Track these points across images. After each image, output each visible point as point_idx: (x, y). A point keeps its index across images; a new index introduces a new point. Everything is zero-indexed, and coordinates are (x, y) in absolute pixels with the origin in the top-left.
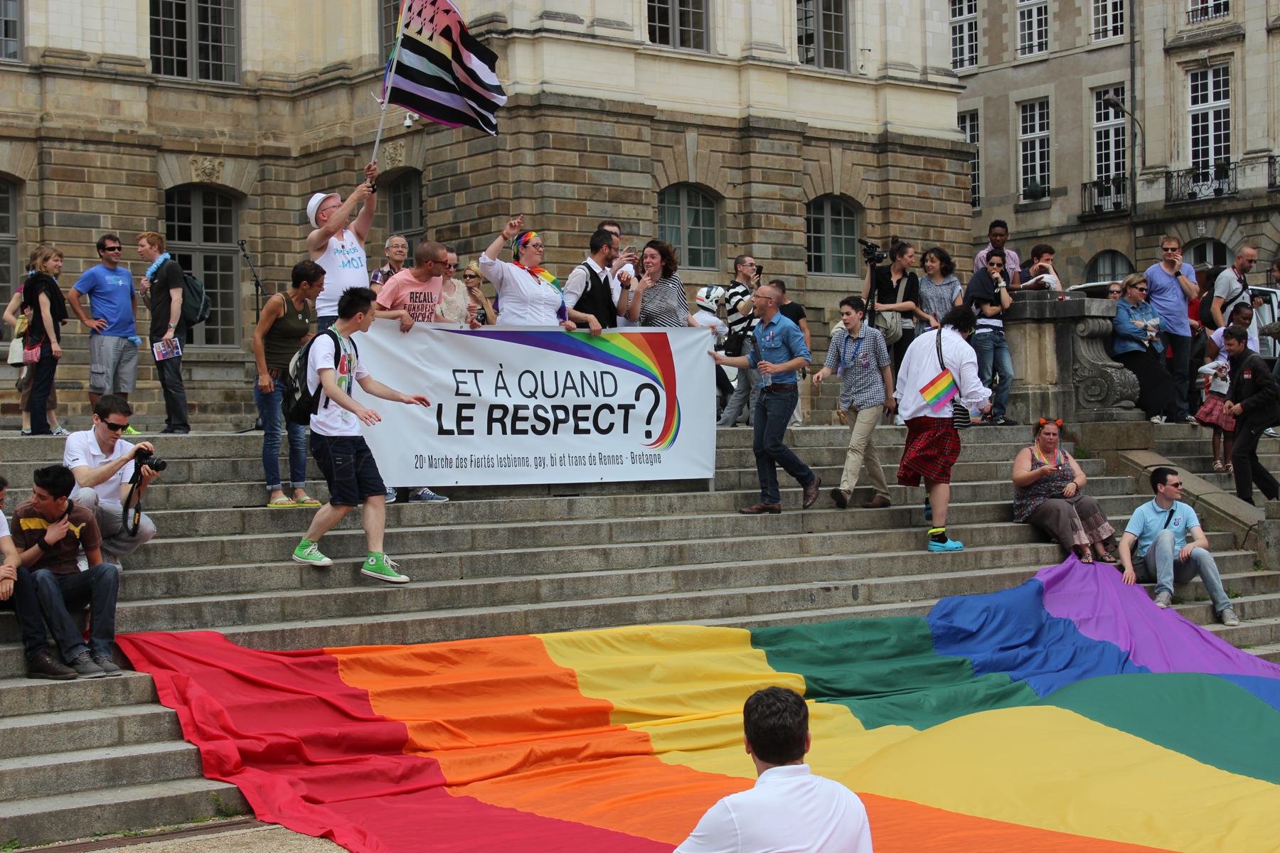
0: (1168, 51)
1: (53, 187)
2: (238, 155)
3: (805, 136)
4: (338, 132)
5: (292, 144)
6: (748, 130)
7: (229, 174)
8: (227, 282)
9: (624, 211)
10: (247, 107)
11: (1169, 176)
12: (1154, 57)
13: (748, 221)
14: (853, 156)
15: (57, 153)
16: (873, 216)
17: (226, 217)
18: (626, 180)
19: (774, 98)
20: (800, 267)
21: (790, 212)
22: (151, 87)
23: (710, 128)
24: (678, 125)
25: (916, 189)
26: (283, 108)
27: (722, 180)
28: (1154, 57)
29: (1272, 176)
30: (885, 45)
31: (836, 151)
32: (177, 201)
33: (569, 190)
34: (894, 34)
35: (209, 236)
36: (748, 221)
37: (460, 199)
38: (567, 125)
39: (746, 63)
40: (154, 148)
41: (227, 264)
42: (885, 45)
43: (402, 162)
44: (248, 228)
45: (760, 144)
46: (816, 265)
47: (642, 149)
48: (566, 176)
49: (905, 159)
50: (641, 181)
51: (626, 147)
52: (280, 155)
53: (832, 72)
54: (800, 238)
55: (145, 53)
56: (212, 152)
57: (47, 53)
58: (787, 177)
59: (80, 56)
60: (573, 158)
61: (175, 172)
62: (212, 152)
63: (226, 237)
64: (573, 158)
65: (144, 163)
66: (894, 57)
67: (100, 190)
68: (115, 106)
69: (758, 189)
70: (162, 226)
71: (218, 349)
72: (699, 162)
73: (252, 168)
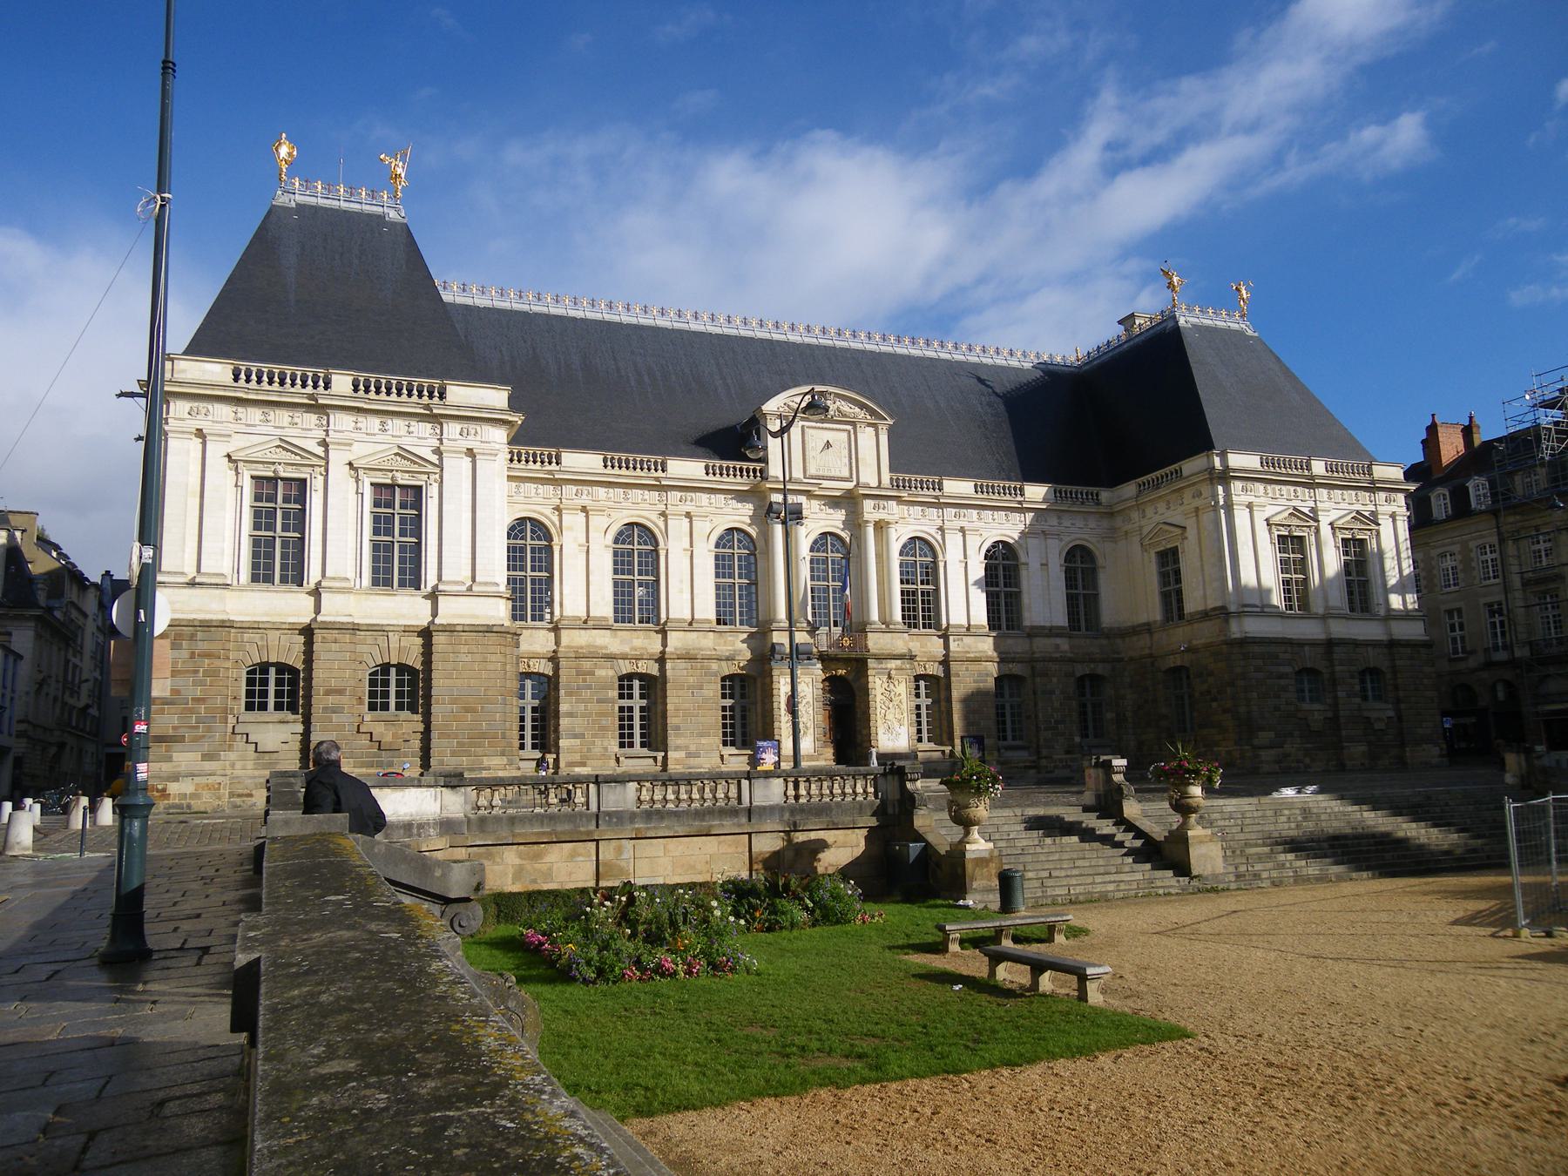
1: (1038, 680)
2: (1103, 661)
4: (1147, 651)
6: (1330, 644)
7: (1100, 669)
9: (1283, 682)
10: (1104, 642)
15: (1039, 666)
16: (1389, 676)
19: (1339, 629)
20: (1358, 700)
21: (1352, 677)
23: (1313, 644)
26: (1119, 641)
35: (1092, 695)
37: (1211, 680)
38: (1257, 649)
39: (1324, 618)
40: (1071, 660)
43: (1179, 663)
46: (1365, 698)
47: (1287, 656)
50: (1288, 669)
52: (1120, 660)
54: (1357, 688)
57: (1032, 628)
59: (1043, 628)
60: (1260, 662)
61: (1081, 670)
62: (1092, 661)
64: (1260, 662)
67: (1055, 680)
68: (1057, 646)
69: (1338, 668)
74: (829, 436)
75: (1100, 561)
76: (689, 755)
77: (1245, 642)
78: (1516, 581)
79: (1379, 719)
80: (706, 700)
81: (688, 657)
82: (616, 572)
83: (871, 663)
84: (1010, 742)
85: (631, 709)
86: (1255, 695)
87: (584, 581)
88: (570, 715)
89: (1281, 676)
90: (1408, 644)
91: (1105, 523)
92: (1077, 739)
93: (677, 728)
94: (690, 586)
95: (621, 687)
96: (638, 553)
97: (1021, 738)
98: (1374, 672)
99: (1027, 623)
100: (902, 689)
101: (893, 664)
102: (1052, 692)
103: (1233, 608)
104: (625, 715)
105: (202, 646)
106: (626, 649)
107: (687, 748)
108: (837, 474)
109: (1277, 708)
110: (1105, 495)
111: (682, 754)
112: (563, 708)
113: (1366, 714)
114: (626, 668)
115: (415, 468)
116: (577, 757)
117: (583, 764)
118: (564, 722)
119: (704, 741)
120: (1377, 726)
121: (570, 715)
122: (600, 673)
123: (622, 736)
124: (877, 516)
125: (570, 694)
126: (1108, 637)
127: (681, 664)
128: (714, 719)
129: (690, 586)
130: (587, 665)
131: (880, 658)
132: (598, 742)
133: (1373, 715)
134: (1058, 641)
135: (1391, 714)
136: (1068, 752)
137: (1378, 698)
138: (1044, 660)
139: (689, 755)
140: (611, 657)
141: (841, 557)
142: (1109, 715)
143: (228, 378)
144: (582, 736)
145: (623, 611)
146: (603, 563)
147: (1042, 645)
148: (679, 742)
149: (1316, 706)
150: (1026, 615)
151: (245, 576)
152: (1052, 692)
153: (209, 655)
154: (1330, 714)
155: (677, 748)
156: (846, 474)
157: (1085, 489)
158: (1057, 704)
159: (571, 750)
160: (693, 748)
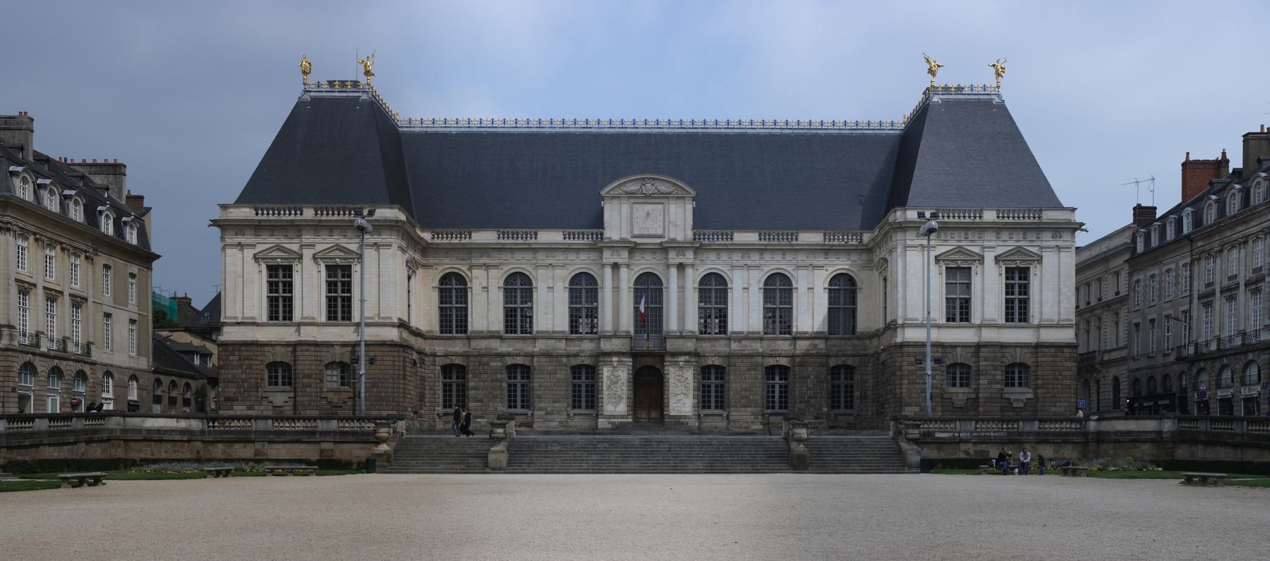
0: (1199, 298)
2: (853, 356)
3: (1003, 346)
5: (870, 351)
6: (979, 346)
7: (850, 362)
10: (856, 342)
11: (1196, 345)
12: (1195, 301)
13: (978, 373)
14: (1024, 350)
17: (852, 373)
21: (995, 369)
22: (827, 339)
23: (965, 346)
24: (953, 346)
26: (867, 342)
27: (970, 361)
28: (1195, 301)
29: (1218, 345)
30: (1041, 313)
31: (1018, 350)
32: (835, 371)
34: (1045, 310)
36: (978, 373)
38: (911, 350)
42: (1041, 313)
44: (857, 377)
45: (983, 350)
48: (910, 364)
49: (1046, 350)
52: (866, 355)
53: (1023, 324)
55: (826, 329)
56: (846, 356)
61: (833, 362)
62: (846, 356)
65: (824, 360)
66: (1045, 317)
71: (849, 411)
72: (960, 356)
73: (858, 359)
74: (649, 207)
75: (859, 284)
77: (902, 345)
78: (1196, 296)
80: (559, 380)
81: (547, 355)
82: (506, 302)
83: (668, 359)
85: (515, 386)
86: (905, 381)
87: (486, 310)
88: (475, 388)
90: (1058, 347)
91: (864, 257)
92: (825, 409)
93: (540, 397)
94: (550, 310)
95: (509, 372)
97: (786, 407)
98: (1023, 366)
100: (689, 374)
101: (683, 358)
103: (900, 321)
104: (512, 389)
106: (511, 349)
107: (545, 409)
108: (652, 232)
112: (471, 384)
113: (1006, 396)
118: (471, 393)
120: (1015, 405)
121: (475, 388)
124: (678, 261)
125: (475, 377)
126: (859, 338)
127: (544, 359)
128: (565, 391)
129: (550, 310)
130: (485, 360)
131: (675, 354)
133: (1012, 397)
134: (816, 342)
135: (1031, 396)
137: (1027, 385)
140: (502, 356)
141: (649, 287)
142: (857, 394)
145: (510, 325)
146: (498, 297)
148: (542, 405)
149: (965, 390)
154: (973, 396)
158: (810, 386)
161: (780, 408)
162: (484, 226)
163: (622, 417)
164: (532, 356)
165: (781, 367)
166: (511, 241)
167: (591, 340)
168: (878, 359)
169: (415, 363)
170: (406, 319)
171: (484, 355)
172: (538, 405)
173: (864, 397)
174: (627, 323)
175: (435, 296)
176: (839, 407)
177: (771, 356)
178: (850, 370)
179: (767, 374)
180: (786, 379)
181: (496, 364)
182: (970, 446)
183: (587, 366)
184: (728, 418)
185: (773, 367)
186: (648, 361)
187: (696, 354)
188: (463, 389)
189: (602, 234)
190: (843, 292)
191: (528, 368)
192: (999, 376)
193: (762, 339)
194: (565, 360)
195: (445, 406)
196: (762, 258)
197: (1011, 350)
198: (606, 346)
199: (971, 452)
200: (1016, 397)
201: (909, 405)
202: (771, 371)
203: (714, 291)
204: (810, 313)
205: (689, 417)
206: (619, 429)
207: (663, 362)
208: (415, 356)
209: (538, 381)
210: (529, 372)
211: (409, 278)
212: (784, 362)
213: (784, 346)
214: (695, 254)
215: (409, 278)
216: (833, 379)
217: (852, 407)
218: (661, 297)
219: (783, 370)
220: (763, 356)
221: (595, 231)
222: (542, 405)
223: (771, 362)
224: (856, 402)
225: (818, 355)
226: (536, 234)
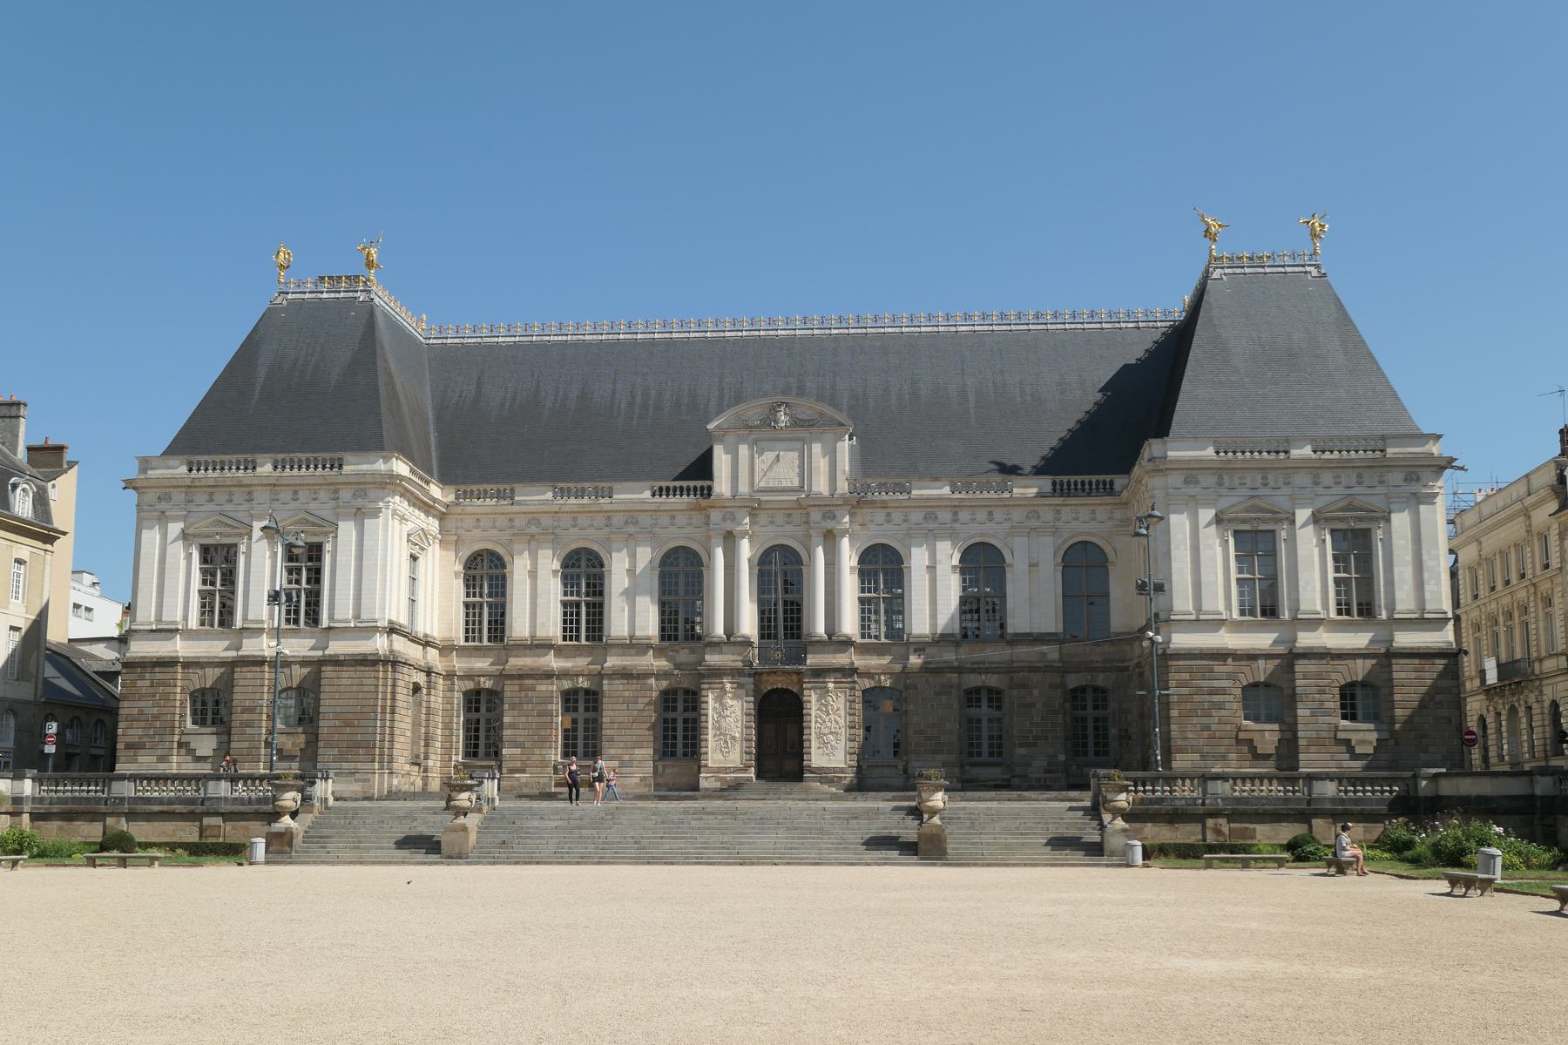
1: (1015, 692)
2: (1104, 670)
7: (1100, 680)
8: (1106, 729)
9: (1216, 698)
17: (1105, 699)
18: (1216, 684)
21: (1322, 692)
25: (1413, 675)
31: (1360, 662)
32: (1077, 694)
33: (1184, 691)
35: (1096, 707)
41: (1105, 719)
44: (1113, 705)
51: (1216, 669)
52: (1126, 669)
55: (1061, 630)
56: (1091, 670)
58: (1319, 676)
60: (1186, 676)
61: (1073, 681)
62: (1091, 670)
63: (1105, 707)
64: (1186, 676)
67: (1036, 692)
70: (1068, 705)
75: (1111, 556)
76: (623, 764)
79: (1363, 742)
81: (626, 675)
84: (985, 757)
88: (513, 726)
89: (1214, 692)
91: (1118, 514)
92: (1062, 757)
96: (585, 573)
99: (1010, 630)
102: (1033, 705)
105: (158, 676)
109: (1207, 728)
110: (1119, 481)
111: (616, 764)
112: (506, 720)
114: (567, 684)
115: (316, 529)
116: (518, 764)
117: (523, 771)
118: (507, 733)
119: (637, 751)
121: (513, 726)
122: (543, 688)
123: (566, 746)
130: (528, 682)
131: (820, 673)
132: (537, 751)
134: (1044, 648)
136: (1047, 772)
138: (1021, 669)
139: (623, 764)
142: (1113, 731)
143: (184, 469)
144: (521, 745)
147: (1023, 652)
148: (613, 751)
150: (1009, 621)
151: (193, 623)
152: (1033, 705)
153: (159, 685)
155: (612, 758)
156: (796, 483)
157: (1094, 478)
159: (512, 758)
160: (626, 758)
161: (991, 754)
162: (534, 476)
163: (737, 770)
164: (601, 675)
165: (990, 690)
166: (573, 501)
167: (693, 651)
168: (1141, 674)
169: (416, 688)
170: (403, 620)
171: (530, 676)
172: (609, 750)
173: (1125, 736)
174: (749, 624)
175: (459, 587)
176: (1086, 753)
177: (973, 671)
178: (1101, 693)
179: (969, 700)
180: (999, 708)
181: (543, 687)
182: (1222, 821)
183: (687, 692)
184: (905, 771)
185: (978, 690)
186: (780, 683)
187: (850, 671)
188: (495, 728)
189: (710, 488)
190: (1084, 568)
191: (595, 693)
192: (1333, 703)
193: (958, 644)
194: (652, 681)
195: (467, 755)
196: (955, 520)
197: (1350, 662)
198: (712, 659)
199: (1226, 830)
200: (1361, 736)
201: (1182, 750)
202: (972, 696)
203: (884, 569)
204: (1034, 603)
205: (842, 770)
206: (732, 789)
207: (800, 683)
208: (421, 678)
209: (611, 713)
210: (596, 701)
211: (414, 558)
212: (993, 681)
213: (996, 654)
214: (852, 515)
215: (414, 558)
216: (1075, 708)
217: (1106, 753)
218: (701, 583)
219: (995, 696)
220: (959, 670)
221: (699, 484)
222: (613, 751)
223: (973, 681)
224: (1114, 745)
225: (1048, 669)
226: (611, 490)
